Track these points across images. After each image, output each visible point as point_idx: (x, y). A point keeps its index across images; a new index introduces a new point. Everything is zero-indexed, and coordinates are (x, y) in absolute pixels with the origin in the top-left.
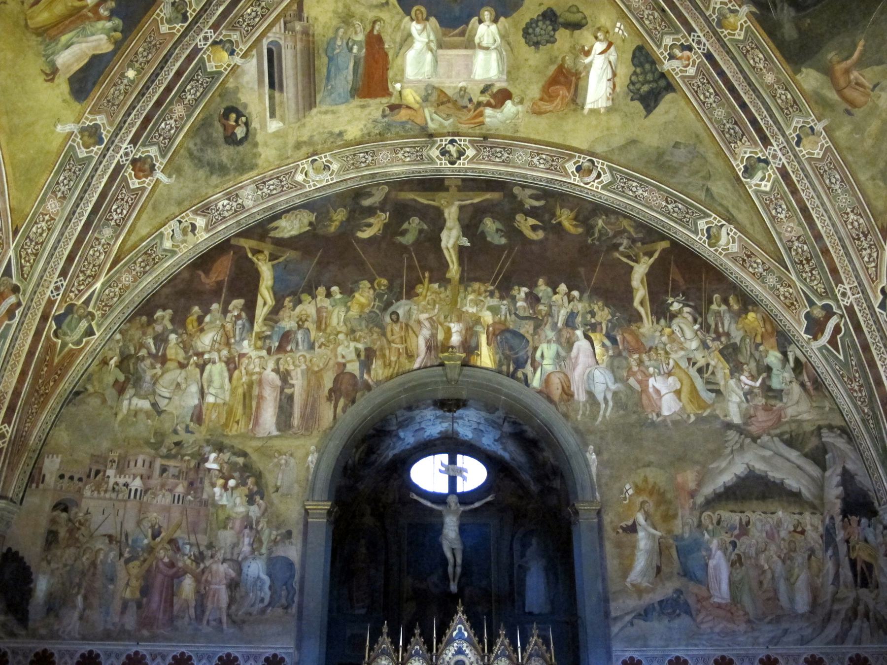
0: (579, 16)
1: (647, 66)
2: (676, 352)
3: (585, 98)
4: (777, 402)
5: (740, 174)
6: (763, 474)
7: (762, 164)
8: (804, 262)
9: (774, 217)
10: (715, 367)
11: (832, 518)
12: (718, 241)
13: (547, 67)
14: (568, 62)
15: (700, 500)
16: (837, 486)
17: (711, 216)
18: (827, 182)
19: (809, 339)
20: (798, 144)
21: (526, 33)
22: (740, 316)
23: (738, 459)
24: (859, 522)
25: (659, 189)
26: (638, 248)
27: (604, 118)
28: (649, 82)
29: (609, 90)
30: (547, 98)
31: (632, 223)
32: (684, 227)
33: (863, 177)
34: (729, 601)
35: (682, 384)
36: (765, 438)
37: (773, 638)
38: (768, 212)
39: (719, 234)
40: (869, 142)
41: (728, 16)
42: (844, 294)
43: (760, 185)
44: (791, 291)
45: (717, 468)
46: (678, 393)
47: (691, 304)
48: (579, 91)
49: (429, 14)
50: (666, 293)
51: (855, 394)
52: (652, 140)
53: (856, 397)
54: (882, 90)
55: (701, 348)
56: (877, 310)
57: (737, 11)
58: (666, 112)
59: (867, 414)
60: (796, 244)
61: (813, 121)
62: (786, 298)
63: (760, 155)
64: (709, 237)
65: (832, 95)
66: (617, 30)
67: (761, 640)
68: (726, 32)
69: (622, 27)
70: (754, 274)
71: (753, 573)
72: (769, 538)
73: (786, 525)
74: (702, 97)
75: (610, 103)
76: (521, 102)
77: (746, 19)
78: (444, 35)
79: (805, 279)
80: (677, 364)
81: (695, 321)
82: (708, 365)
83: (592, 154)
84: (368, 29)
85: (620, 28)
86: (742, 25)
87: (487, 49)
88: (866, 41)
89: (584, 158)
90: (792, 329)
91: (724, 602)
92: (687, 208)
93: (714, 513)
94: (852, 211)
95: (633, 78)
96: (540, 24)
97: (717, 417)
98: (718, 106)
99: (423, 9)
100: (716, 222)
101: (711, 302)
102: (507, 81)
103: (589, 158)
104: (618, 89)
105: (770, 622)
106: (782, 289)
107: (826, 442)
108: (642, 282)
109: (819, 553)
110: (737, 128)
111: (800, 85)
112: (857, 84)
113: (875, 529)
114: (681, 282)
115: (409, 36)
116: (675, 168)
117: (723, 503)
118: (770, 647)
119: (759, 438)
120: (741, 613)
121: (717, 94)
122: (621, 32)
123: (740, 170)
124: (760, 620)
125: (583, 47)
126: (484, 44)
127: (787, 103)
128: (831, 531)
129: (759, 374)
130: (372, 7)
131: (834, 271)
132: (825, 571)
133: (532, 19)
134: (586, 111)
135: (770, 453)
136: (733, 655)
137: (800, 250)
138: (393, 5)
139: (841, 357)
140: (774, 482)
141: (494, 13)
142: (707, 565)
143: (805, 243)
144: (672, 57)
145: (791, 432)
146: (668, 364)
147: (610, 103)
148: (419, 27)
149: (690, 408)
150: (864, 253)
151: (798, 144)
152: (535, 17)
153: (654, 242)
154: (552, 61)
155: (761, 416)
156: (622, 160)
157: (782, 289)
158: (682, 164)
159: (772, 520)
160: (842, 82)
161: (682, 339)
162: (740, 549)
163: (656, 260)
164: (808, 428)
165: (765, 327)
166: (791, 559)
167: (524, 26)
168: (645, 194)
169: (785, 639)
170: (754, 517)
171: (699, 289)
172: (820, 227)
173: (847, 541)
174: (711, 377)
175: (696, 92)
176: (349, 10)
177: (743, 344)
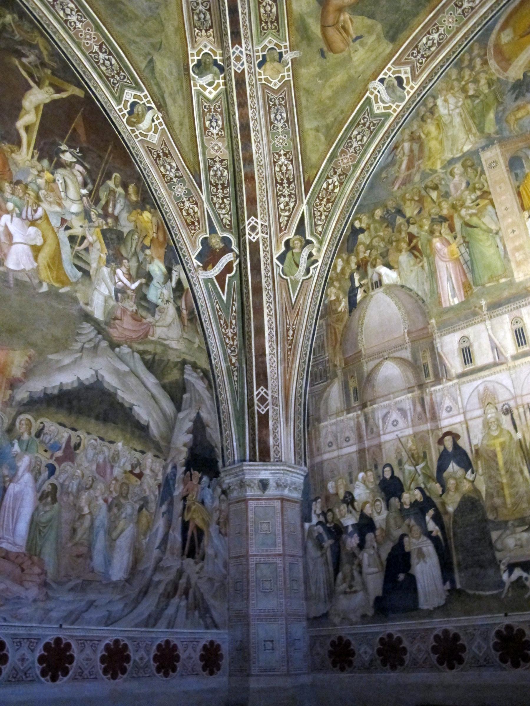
2: (50, 203)
4: (149, 315)
5: (191, 66)
6: (112, 390)
7: (216, 69)
8: (220, 187)
9: (206, 129)
10: (91, 244)
11: (175, 467)
12: (139, 122)
15: (22, 395)
16: (188, 432)
17: (143, 91)
18: (273, 116)
19: (199, 266)
20: (260, 65)
22: (135, 209)
23: (86, 361)
24: (201, 479)
26: (45, 74)
31: (50, 49)
32: (107, 86)
33: (309, 125)
34: (23, 550)
35: (45, 241)
36: (125, 350)
37: (71, 613)
38: (202, 120)
39: (143, 116)
40: (328, 92)
42: (253, 229)
43: (205, 89)
44: (196, 209)
45: (58, 361)
46: (36, 250)
47: (87, 165)
50: (63, 138)
51: (227, 341)
53: (227, 344)
54: (362, 45)
55: (83, 215)
56: (275, 261)
59: (233, 364)
60: (218, 165)
61: (286, 47)
62: (188, 214)
63: (218, 58)
64: (131, 113)
65: (315, 28)
67: (54, 615)
70: (164, 175)
71: (66, 515)
72: (99, 473)
73: (123, 461)
79: (215, 204)
80: (46, 217)
81: (85, 185)
82: (84, 238)
90: (185, 249)
91: (15, 549)
92: (121, 68)
93: (36, 419)
94: (285, 155)
97: (75, 300)
100: (145, 101)
101: (108, 177)
105: (72, 590)
106: (187, 204)
107: (187, 380)
108: (37, 108)
109: (152, 506)
110: (208, 17)
112: (343, 27)
113: (214, 490)
114: (83, 137)
117: (52, 409)
118: (64, 626)
119: (119, 346)
120: (37, 570)
123: (193, 61)
124: (60, 584)
127: (269, 16)
128: (171, 482)
129: (138, 277)
131: (252, 201)
132: (154, 530)
135: (127, 369)
136: (6, 635)
137: (219, 173)
139: (224, 298)
140: (122, 405)
142: (5, 490)
143: (227, 168)
145: (155, 354)
146: (36, 211)
149: (45, 274)
150: (282, 199)
151: (260, 65)
153: (68, 82)
155: (127, 323)
157: (187, 204)
158: (137, 17)
159: (107, 451)
160: (331, 19)
161: (63, 194)
162: (60, 478)
163: (63, 99)
164: (173, 357)
165: (157, 233)
166: (119, 506)
169: (87, 616)
170: (87, 441)
171: (101, 157)
172: (254, 151)
173: (184, 499)
174: (83, 252)
177: (130, 237)
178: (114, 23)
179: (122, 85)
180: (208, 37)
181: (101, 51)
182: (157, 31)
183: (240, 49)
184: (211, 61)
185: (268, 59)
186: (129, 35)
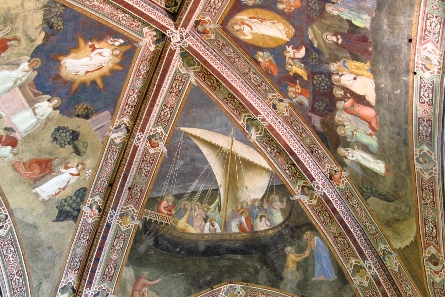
0: (84, 150)
1: (79, 200)
3: (41, 185)
5: (60, 287)
13: (45, 153)
14: (56, 162)
21: (58, 130)
25: (21, 262)
27: (37, 202)
28: (71, 207)
29: (54, 194)
30: (27, 167)
41: (129, 217)
48: (43, 179)
49: (37, 69)
52: (43, 235)
57: (135, 219)
58: (63, 228)
61: (111, 291)
65: (130, 288)
66: (87, 172)
68: (120, 221)
69: (90, 174)
74: (82, 236)
75: (47, 199)
76: (15, 154)
77: (134, 225)
78: (30, 85)
83: (11, 214)
84: (8, 37)
85: (89, 173)
86: (129, 226)
87: (35, 114)
88: (162, 280)
89: (5, 212)
92: (23, 285)
95: (69, 199)
96: (68, 133)
98: (83, 246)
99: (39, 65)
102: (23, 138)
103: (8, 214)
104: (57, 196)
110: (79, 264)
111: (122, 272)
112: (143, 294)
115: (18, 65)
116: (38, 259)
121: (87, 241)
122: (87, 175)
125: (69, 163)
126: (37, 111)
130: (25, 32)
133: (68, 127)
134: (34, 191)
138: (34, 45)
141: (59, 105)
144: (91, 207)
147: (47, 199)
148: (27, 68)
152: (70, 129)
154: (51, 154)
156: (20, 231)
160: (138, 287)
167: (61, 126)
168: (11, 259)
175: (82, 231)
176: (15, 19)
178: (30, 261)
179: (20, 294)
180: (74, 274)
181: (16, 274)
182: (50, 268)
183: (89, 290)
184: (71, 286)
185: (100, 294)
186: (35, 269)
